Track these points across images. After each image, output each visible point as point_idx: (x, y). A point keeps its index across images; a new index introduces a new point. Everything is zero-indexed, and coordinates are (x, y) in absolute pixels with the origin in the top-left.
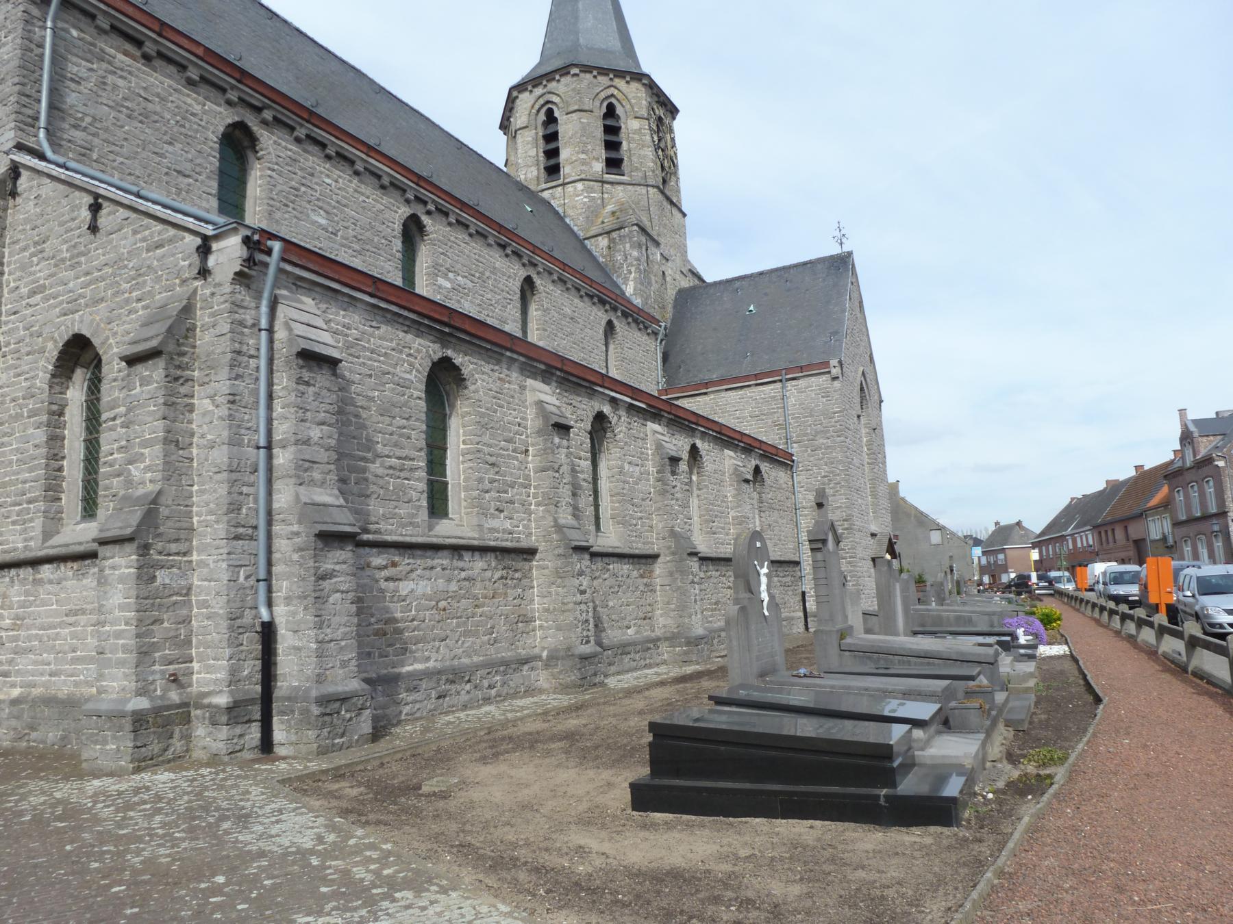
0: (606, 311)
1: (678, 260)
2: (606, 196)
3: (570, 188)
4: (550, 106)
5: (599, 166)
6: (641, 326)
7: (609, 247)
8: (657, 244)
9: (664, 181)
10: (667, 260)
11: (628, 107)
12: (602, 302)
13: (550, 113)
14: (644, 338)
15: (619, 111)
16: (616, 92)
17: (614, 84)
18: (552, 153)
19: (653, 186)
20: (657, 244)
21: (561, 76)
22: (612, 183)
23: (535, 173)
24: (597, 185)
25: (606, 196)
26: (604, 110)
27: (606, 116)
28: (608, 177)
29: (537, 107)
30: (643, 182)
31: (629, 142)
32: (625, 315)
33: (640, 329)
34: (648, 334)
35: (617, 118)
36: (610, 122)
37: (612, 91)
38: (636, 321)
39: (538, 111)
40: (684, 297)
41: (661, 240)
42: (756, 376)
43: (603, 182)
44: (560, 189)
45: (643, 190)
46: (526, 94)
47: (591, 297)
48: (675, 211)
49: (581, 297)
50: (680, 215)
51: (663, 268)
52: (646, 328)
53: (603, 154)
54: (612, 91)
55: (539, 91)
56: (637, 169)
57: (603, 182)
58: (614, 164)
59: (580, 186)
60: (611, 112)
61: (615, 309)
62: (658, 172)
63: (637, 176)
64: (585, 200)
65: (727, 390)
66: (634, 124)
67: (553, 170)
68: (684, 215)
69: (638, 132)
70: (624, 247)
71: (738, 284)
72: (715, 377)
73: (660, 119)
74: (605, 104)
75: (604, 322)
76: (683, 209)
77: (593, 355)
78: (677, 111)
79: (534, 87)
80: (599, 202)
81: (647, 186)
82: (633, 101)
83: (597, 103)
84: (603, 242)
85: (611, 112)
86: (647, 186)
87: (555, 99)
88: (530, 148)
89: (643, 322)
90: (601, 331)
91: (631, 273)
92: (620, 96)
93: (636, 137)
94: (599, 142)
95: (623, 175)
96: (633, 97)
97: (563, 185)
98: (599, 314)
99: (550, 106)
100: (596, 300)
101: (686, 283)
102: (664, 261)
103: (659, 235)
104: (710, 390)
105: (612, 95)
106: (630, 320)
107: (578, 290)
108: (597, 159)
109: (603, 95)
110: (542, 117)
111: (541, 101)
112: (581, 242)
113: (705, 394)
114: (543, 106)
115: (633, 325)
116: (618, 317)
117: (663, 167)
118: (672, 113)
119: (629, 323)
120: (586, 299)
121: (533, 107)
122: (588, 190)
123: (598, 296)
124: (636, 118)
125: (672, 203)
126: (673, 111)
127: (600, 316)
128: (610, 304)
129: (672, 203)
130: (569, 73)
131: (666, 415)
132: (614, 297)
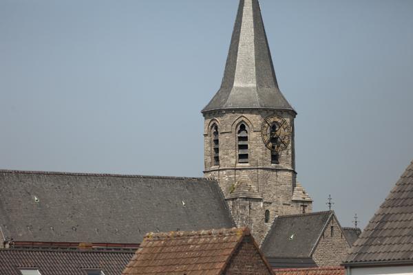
2: (237, 176)
3: (221, 172)
11: (250, 126)
16: (244, 119)
24: (233, 172)
25: (237, 176)
26: (239, 128)
28: (239, 165)
36: (243, 134)
37: (242, 118)
39: (212, 127)
45: (256, 171)
58: (243, 157)
59: (225, 172)
69: (255, 139)
80: (233, 179)
83: (234, 127)
84: (231, 202)
92: (246, 121)
93: (254, 142)
97: (219, 170)
108: (233, 157)
109: (237, 122)
112: (223, 203)
122: (229, 174)
124: (254, 131)
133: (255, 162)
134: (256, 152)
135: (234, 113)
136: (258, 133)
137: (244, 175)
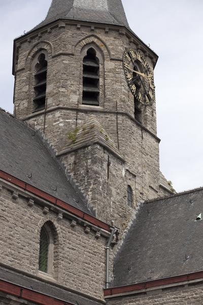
0: (45, 213)
1: (147, 178)
2: (79, 121)
3: (50, 116)
4: (43, 52)
5: (75, 98)
6: (88, 230)
7: (75, 163)
8: (123, 162)
9: (137, 112)
10: (135, 176)
11: (105, 51)
12: (42, 205)
13: (43, 56)
14: (90, 241)
15: (98, 55)
16: (96, 40)
17: (95, 34)
18: (41, 89)
19: (123, 114)
20: (123, 162)
21: (51, 29)
22: (86, 112)
23: (26, 105)
24: (72, 114)
26: (85, 53)
27: (85, 59)
29: (32, 54)
30: (114, 110)
31: (104, 79)
32: (66, 217)
33: (86, 233)
34: (97, 238)
35: (95, 60)
36: (90, 64)
37: (92, 39)
38: (81, 225)
39: (33, 57)
40: (148, 207)
41: (126, 158)
42: (188, 277)
43: (78, 110)
44: (42, 117)
45: (114, 118)
46: (26, 44)
47: (27, 199)
48: (146, 136)
49: (14, 198)
50: (153, 140)
51: (130, 183)
52: (95, 232)
53: (81, 88)
54: (92, 39)
55: (35, 42)
56: (109, 100)
57: (78, 110)
58: (90, 97)
59: (58, 114)
60: (91, 56)
61: (56, 212)
62: (131, 103)
63: (109, 106)
64: (61, 125)
65: (163, 289)
66: (109, 65)
67: (40, 102)
68: (158, 140)
69: (113, 71)
70: (87, 163)
71: (193, 196)
72: (155, 278)
73: (137, 61)
74: (86, 50)
75: (41, 223)
76: (158, 136)
77: (22, 251)
78: (157, 57)
79: (32, 38)
81: (117, 113)
82: (110, 47)
84: (71, 159)
85: (91, 56)
86: (117, 113)
87: (45, 47)
88: (28, 89)
89: (90, 226)
90: (37, 230)
91: (90, 184)
92: (99, 43)
93: (111, 74)
94: (77, 79)
95: (98, 105)
96: (115, 45)
97: (45, 113)
98: (36, 215)
99: (43, 52)
100: (32, 202)
101: (152, 196)
102: (131, 177)
103: (124, 154)
104: (148, 290)
105: (93, 42)
106: (74, 223)
107: (12, 192)
108: (75, 92)
109: (84, 42)
110: (36, 61)
111: (36, 49)
113: (145, 293)
114: (37, 52)
115: (78, 228)
116: (59, 220)
117: (136, 101)
118: (151, 58)
119: (73, 226)
120: (20, 201)
121: (29, 54)
122: (66, 117)
123: (34, 199)
124: (112, 60)
125: (144, 129)
126: (153, 57)
127: (39, 218)
128: (49, 207)
129: (144, 129)
130: (57, 26)
131: (14, 299)
132: (54, 201)
133: (112, 104)
134: (116, 90)
135: (78, 29)
136: (118, 63)
137: (94, 120)
